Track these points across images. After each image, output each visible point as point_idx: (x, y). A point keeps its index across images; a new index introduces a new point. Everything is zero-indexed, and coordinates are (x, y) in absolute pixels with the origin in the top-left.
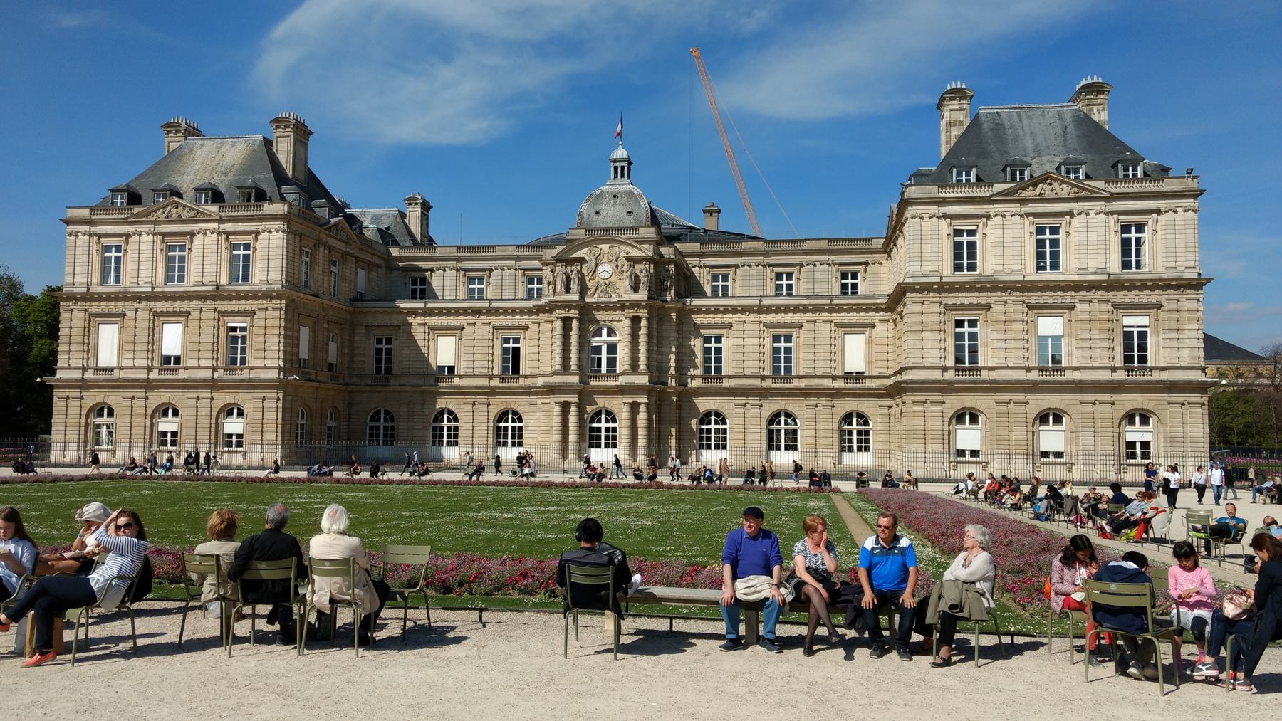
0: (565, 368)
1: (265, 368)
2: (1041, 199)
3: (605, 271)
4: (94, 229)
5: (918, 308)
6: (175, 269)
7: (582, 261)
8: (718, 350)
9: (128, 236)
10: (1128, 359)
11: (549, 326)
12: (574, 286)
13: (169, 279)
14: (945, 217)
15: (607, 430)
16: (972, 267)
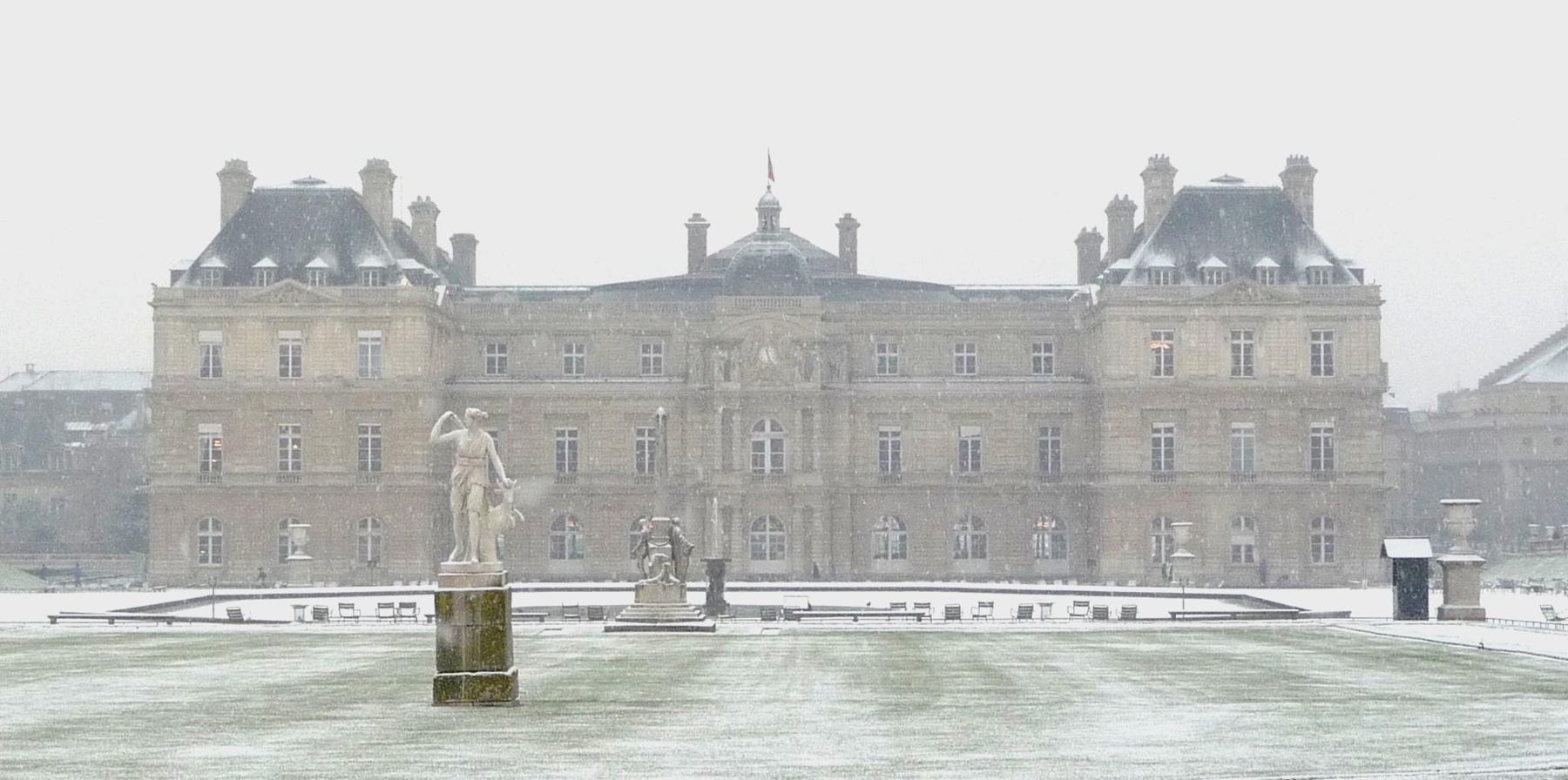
0: (727, 469)
1: (409, 475)
2: (1236, 302)
3: (767, 356)
4: (189, 313)
5: (1114, 414)
6: (290, 362)
7: (738, 343)
8: (896, 445)
9: (229, 319)
10: (1316, 464)
11: (699, 418)
12: (735, 373)
13: (284, 373)
14: (1143, 320)
15: (772, 539)
16: (1169, 371)
